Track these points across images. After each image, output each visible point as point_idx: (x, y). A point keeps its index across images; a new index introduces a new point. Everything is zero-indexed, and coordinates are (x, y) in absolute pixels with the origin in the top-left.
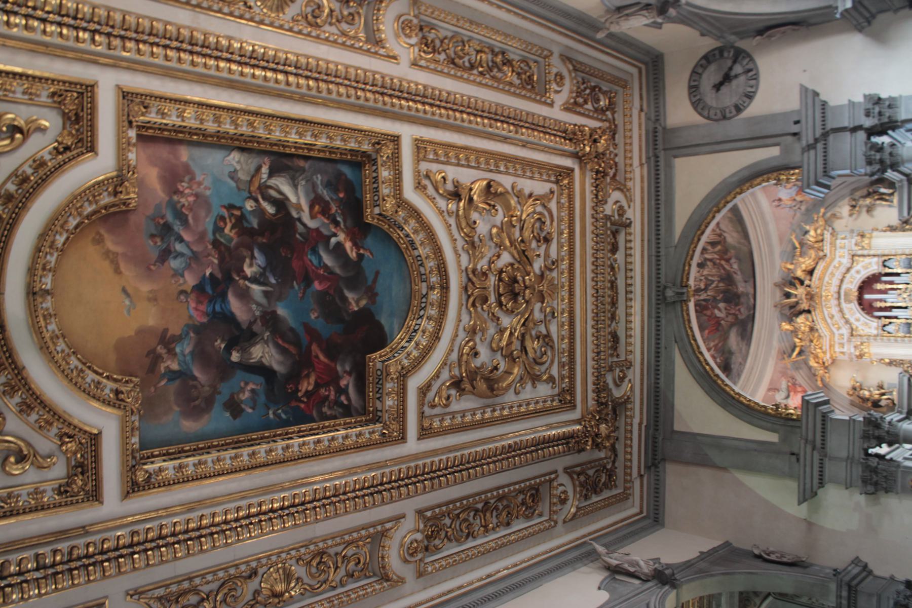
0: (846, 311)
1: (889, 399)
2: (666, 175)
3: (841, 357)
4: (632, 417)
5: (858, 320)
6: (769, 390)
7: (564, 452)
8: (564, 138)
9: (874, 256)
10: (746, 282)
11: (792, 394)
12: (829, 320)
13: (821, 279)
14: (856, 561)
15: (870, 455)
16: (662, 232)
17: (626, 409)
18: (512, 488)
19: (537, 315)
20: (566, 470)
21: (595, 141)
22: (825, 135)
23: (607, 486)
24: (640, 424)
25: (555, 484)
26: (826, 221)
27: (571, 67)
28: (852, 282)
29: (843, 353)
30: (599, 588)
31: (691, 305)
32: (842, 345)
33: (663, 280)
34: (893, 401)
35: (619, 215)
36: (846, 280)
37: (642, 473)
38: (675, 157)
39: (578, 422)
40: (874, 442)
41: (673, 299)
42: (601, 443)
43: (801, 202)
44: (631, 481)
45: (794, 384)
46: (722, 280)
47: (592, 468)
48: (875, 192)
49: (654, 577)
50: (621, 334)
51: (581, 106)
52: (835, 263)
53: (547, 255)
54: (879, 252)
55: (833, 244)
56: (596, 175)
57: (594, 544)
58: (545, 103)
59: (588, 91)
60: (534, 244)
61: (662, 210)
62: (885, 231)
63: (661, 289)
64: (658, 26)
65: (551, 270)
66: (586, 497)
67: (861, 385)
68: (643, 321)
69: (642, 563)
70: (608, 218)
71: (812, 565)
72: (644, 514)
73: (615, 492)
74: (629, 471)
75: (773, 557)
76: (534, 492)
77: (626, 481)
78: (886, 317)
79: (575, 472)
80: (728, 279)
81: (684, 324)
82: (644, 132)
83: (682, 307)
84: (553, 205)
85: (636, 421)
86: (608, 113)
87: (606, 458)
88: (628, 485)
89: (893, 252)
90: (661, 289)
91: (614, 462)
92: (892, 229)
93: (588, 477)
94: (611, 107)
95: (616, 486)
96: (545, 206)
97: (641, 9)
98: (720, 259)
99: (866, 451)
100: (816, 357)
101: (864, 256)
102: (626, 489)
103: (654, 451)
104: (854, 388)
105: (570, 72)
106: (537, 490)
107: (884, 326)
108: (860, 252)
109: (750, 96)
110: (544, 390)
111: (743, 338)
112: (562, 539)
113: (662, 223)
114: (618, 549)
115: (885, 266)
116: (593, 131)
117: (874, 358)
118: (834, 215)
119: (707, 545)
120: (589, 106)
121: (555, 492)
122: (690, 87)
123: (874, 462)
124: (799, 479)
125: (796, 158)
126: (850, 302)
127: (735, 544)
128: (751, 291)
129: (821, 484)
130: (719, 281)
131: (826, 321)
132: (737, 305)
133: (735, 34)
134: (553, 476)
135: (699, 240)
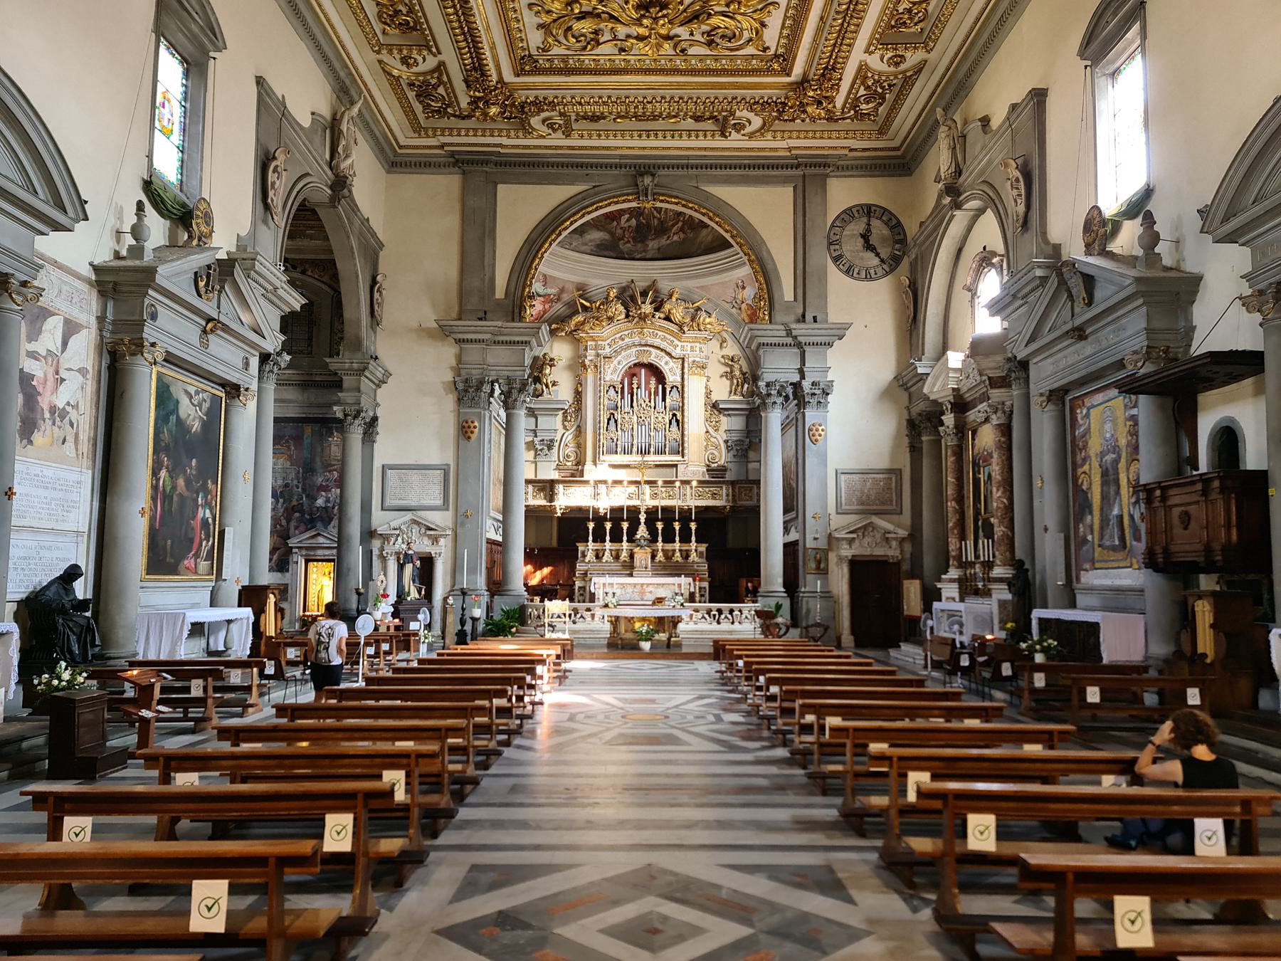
2: (775, 176)
3: (582, 347)
4: (509, 137)
6: (545, 276)
7: (465, 65)
8: (826, 68)
9: (683, 378)
10: (659, 249)
11: (542, 299)
13: (661, 328)
14: (388, 374)
15: (492, 385)
16: (714, 172)
17: (517, 130)
18: (420, 14)
19: (622, 31)
20: (442, 64)
21: (820, 103)
22: (799, 345)
23: (426, 107)
24: (500, 145)
25: (425, 53)
27: (908, 74)
29: (586, 349)
30: (313, 114)
31: (634, 204)
32: (596, 348)
33: (661, 172)
34: (541, 395)
35: (735, 124)
36: (658, 352)
37: (446, 148)
38: (795, 188)
39: (500, 80)
40: (505, 388)
41: (640, 184)
42: (478, 107)
44: (435, 136)
45: (552, 301)
46: (661, 222)
47: (446, 91)
49: (337, 176)
50: (602, 124)
51: (863, 83)
52: (676, 342)
53: (694, 43)
54: (686, 383)
55: (696, 340)
56: (781, 103)
57: (361, 102)
58: (870, 44)
59: (880, 90)
60: (705, 28)
61: (738, 172)
63: (652, 169)
64: (938, 180)
65: (675, 47)
66: (411, 85)
68: (617, 148)
69: (349, 161)
70: (732, 113)
71: (375, 333)
72: (399, 151)
73: (421, 116)
74: (447, 133)
75: (376, 295)
76: (412, 24)
77: (435, 129)
78: (623, 388)
79: (441, 74)
80: (662, 230)
81: (614, 197)
82: (826, 153)
83: (632, 194)
84: (750, 50)
85: (505, 141)
86: (852, 112)
87: (460, 109)
88: (430, 133)
89: (686, 395)
90: (652, 169)
91: (455, 116)
92: (708, 394)
93: (435, 87)
94: (860, 116)
95: (427, 118)
96: (751, 40)
97: (957, 165)
98: (683, 221)
99: (497, 381)
100: (583, 323)
102: (426, 129)
103: (472, 162)
104: (552, 360)
105: (904, 72)
106: (414, 29)
108: (686, 365)
109: (848, 272)
110: (535, 39)
111: (598, 246)
112: (362, 60)
113: (724, 172)
114: (359, 129)
116: (831, 100)
118: (724, 341)
119: (377, 225)
120: (862, 91)
121: (415, 52)
122: (869, 206)
123: (487, 388)
124: (460, 319)
125: (779, 317)
127: (381, 254)
128: (649, 256)
129: (458, 341)
130: (659, 219)
132: (634, 239)
133: (916, 258)
134: (434, 50)
135: (704, 214)
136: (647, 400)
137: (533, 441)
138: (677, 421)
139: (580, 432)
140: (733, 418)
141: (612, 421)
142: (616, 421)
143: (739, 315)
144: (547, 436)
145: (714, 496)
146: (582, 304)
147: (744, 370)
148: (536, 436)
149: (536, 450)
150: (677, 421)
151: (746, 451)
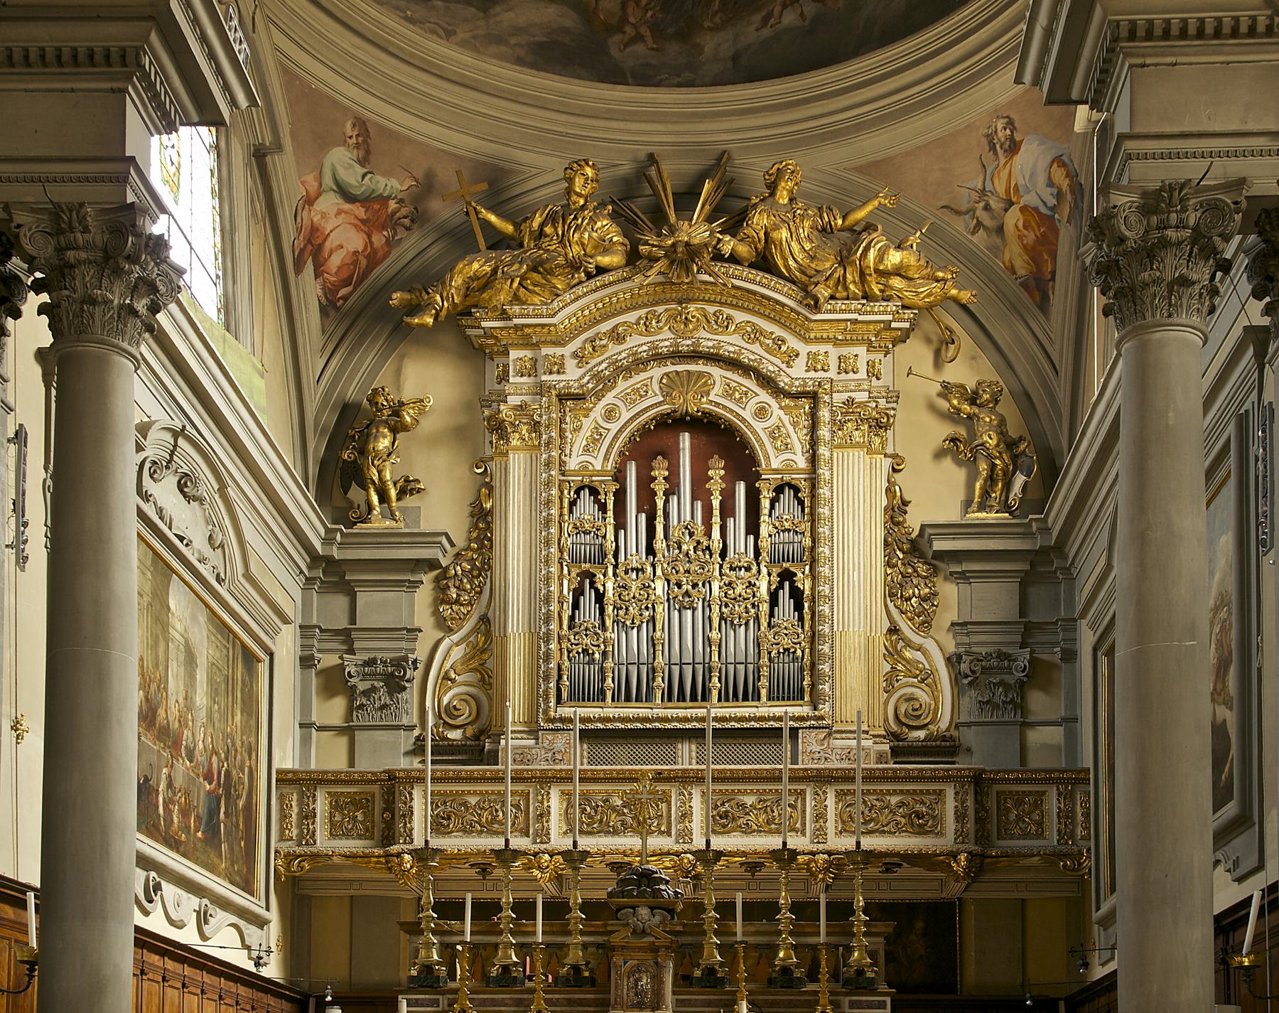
0: (637, 378)
1: (370, 508)
5: (609, 414)
9: (813, 459)
11: (361, 212)
12: (606, 327)
26: (929, 308)
28: (729, 394)
32: (532, 369)
43: (1000, 230)
45: (392, 222)
48: (1014, 458)
52: (793, 342)
54: (824, 472)
62: (888, 490)
67: (405, 428)
78: (620, 496)
89: (824, 511)
101: (814, 428)
107: (594, 492)
108: (824, 414)
115: (779, 490)
117: (492, 466)
126: (667, 393)
131: (605, 318)
136: (700, 527)
137: (341, 667)
138: (796, 595)
139: (488, 635)
140: (978, 587)
141: (589, 596)
142: (600, 598)
143: (996, 251)
144: (385, 650)
145: (920, 823)
146: (486, 224)
147: (1013, 433)
148: (351, 651)
149: (351, 692)
150: (796, 595)
151: (1022, 686)
